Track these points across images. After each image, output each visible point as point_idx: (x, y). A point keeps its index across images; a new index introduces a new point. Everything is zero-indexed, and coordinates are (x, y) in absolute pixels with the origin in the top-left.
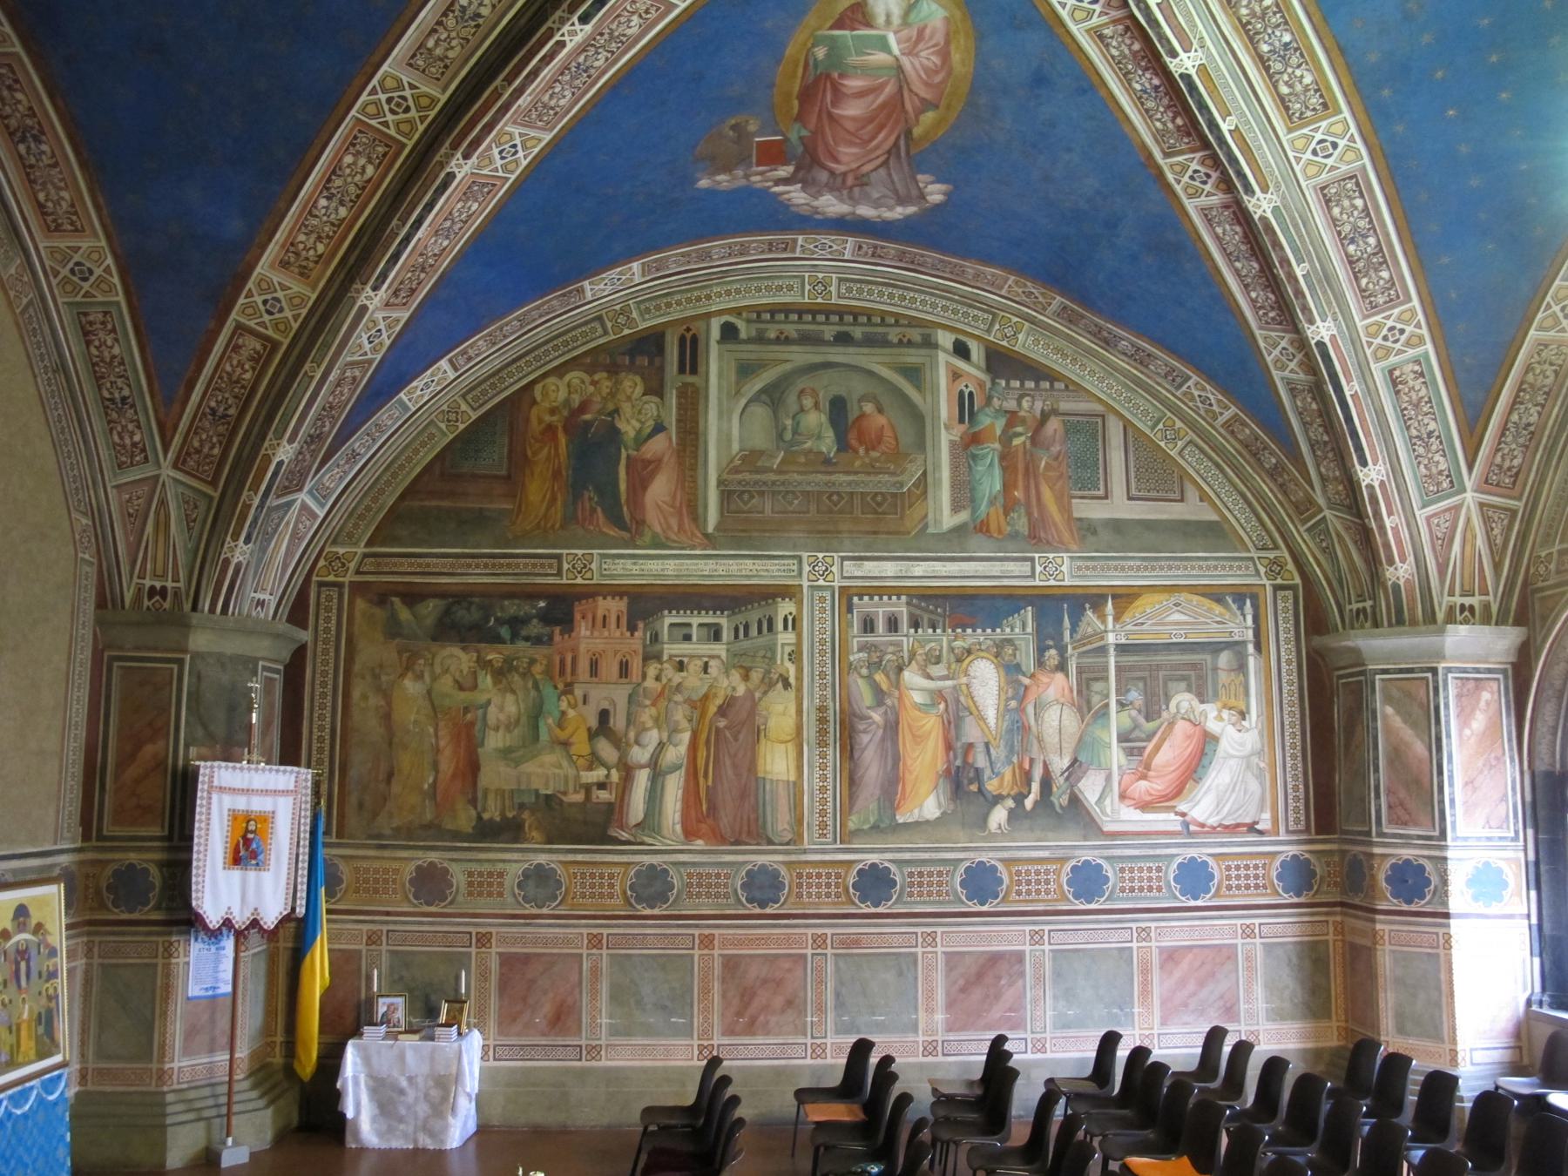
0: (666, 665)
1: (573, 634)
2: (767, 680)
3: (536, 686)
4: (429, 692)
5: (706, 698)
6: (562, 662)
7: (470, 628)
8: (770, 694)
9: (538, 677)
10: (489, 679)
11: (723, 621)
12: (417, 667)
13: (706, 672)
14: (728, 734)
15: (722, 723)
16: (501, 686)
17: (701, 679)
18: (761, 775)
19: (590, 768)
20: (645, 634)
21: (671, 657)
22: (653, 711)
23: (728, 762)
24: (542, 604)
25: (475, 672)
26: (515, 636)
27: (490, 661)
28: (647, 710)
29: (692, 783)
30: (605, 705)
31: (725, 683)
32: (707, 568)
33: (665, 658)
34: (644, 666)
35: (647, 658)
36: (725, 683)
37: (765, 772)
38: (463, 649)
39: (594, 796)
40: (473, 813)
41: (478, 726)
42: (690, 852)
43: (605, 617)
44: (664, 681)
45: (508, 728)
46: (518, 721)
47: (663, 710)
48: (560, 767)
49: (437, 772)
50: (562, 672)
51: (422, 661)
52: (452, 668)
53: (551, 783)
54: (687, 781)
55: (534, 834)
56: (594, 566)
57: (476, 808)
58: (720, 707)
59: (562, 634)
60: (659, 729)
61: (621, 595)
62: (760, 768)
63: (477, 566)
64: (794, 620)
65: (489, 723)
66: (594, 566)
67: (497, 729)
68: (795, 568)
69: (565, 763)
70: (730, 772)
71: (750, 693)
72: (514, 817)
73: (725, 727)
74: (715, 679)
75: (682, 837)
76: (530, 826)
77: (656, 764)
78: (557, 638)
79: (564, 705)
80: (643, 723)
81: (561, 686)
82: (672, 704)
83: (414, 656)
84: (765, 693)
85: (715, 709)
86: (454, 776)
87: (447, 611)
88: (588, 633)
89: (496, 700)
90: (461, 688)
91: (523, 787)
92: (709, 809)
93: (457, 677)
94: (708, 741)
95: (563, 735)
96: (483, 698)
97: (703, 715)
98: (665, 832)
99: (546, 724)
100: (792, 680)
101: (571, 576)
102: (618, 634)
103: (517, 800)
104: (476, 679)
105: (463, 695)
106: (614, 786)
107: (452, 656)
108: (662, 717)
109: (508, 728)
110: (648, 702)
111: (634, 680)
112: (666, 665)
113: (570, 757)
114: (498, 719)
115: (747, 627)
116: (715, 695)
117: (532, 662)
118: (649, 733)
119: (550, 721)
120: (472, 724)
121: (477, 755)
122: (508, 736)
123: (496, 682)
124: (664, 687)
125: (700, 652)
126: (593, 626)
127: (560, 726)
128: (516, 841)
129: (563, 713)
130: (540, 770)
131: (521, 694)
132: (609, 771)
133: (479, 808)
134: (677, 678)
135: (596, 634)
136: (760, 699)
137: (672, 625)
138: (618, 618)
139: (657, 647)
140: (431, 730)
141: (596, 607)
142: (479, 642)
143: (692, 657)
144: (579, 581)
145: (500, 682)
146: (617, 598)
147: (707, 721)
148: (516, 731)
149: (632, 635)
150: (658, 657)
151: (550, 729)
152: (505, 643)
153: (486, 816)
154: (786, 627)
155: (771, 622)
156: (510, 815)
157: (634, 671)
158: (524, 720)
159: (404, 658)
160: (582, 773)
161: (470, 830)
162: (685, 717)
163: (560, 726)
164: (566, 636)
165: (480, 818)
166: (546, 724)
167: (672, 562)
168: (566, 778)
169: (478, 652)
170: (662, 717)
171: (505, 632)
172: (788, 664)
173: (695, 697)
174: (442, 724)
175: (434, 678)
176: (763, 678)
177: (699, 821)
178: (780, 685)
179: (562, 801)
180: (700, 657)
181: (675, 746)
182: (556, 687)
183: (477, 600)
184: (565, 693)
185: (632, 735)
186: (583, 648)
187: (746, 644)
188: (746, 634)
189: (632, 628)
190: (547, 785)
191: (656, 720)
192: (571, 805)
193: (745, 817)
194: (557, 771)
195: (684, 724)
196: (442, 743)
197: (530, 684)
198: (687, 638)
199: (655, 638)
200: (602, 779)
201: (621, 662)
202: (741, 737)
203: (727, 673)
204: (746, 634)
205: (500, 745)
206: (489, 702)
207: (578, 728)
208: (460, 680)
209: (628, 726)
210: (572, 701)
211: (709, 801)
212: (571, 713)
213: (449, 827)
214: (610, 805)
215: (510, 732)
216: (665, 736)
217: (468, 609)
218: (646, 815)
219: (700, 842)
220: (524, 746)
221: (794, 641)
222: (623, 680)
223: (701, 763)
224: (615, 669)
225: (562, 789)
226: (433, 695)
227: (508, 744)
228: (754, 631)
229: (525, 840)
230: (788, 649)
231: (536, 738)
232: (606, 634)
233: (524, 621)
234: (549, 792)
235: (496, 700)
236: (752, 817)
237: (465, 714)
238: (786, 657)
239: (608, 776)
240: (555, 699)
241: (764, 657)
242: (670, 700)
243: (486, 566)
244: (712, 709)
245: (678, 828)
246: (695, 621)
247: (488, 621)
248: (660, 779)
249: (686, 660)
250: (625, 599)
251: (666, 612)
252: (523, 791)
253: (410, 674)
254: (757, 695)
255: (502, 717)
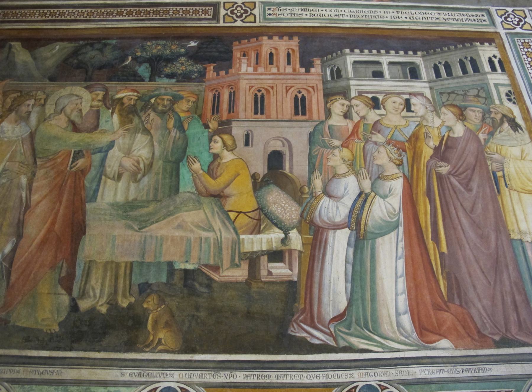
0: (354, 102)
1: (232, 71)
2: (488, 121)
3: (180, 126)
4: (32, 136)
5: (415, 138)
6: (217, 100)
7: (100, 68)
8: (497, 135)
9: (182, 115)
10: (116, 118)
11: (418, 60)
12: (24, 109)
13: (409, 110)
14: (453, 180)
15: (445, 169)
16: (128, 126)
17: (404, 117)
18: (515, 236)
19: (257, 230)
20: (324, 70)
21: (360, 94)
22: (346, 153)
23: (465, 221)
24: (193, 44)
25: (98, 112)
26: (155, 74)
27: (121, 99)
28: (336, 151)
29: (417, 250)
30: (277, 146)
31: (437, 122)
32: (389, 15)
33: (353, 94)
34: (326, 103)
35: (328, 95)
36: (437, 122)
37: (520, 232)
38: (87, 88)
39: (264, 272)
40: (65, 299)
41: (92, 173)
42: (432, 361)
43: (271, 55)
44: (356, 119)
45: (135, 177)
46: (151, 165)
47: (359, 153)
48: (210, 229)
49: (19, 236)
50: (216, 108)
51: (32, 102)
52: (68, 110)
53: (195, 253)
54: (409, 245)
55: (161, 335)
56: (256, 12)
57: (69, 290)
58: (437, 149)
59: (217, 70)
60: (357, 175)
61: (291, 36)
62: (512, 226)
63: (120, 14)
64: (500, 62)
65: (108, 170)
66: (256, 12)
67: (119, 176)
68: (485, 18)
69: (217, 224)
70: (471, 233)
71: (472, 134)
72: (130, 306)
73: (449, 173)
74: (423, 117)
75: (415, 335)
76: (156, 322)
77: (358, 223)
78: (211, 73)
79: (217, 146)
80: (333, 167)
81: (213, 125)
82: (370, 146)
83: (24, 95)
84: (491, 134)
85: (431, 152)
86: (44, 242)
87: (76, 53)
88: (251, 70)
89: (121, 141)
90: (76, 128)
91: (148, 259)
92: (449, 288)
93: (73, 117)
94: (429, 193)
95: (213, 185)
96: (104, 140)
97: (416, 157)
98: (386, 328)
99: (191, 170)
100: (519, 120)
101: (228, 19)
102: (289, 69)
103: (137, 280)
104: (98, 119)
105: (76, 137)
106: (296, 255)
107: (71, 95)
108: (360, 161)
109: (135, 177)
110: (336, 143)
111: (315, 117)
112: (354, 102)
113: (226, 213)
114: (121, 165)
115: (447, 67)
116: (427, 136)
117: (176, 99)
118: (343, 181)
119: (196, 166)
120: (83, 172)
121: (84, 213)
122: (133, 186)
123: (122, 124)
124: (356, 126)
125: (399, 89)
126: (257, 62)
127: (211, 172)
128: (130, 346)
129: (216, 156)
130: (178, 233)
131: (157, 135)
132: (286, 232)
133: (75, 294)
134: (373, 116)
135: (261, 70)
136: (487, 141)
137: (355, 62)
138: (289, 55)
139: (342, 83)
140: (24, 180)
141: (261, 46)
142: (110, 79)
143: (388, 94)
144: (239, 23)
145: (131, 122)
146: (286, 38)
147: (423, 167)
148: (146, 180)
149: (308, 71)
150: (345, 93)
151: (195, 175)
152: (143, 80)
153: (84, 305)
154: (493, 68)
155: (473, 62)
156: (124, 303)
157: (314, 107)
158: (159, 165)
159: (9, 101)
160: (242, 237)
161: (56, 328)
162: (391, 160)
163: (211, 172)
164: (222, 73)
165: (74, 307)
166: (191, 170)
167: (347, 10)
168: (219, 245)
169: (106, 90)
170: (360, 161)
171: (143, 70)
172: (510, 105)
173: (401, 138)
174: (40, 173)
175: (43, 119)
176: (483, 119)
177: (438, 308)
178: (506, 125)
179: (210, 279)
180: (398, 94)
181: (384, 197)
182: (207, 126)
183: (114, 42)
184: (218, 132)
185: (318, 183)
186: (243, 84)
187: (451, 83)
188: (449, 73)
189: (307, 65)
190: (187, 256)
191: (352, 165)
192: (227, 285)
193: (509, 300)
194: (204, 234)
195: (392, 169)
196: (35, 198)
197: (171, 123)
198: (378, 75)
199: (338, 74)
200: (276, 245)
201: (296, 98)
202: (474, 185)
203: (437, 112)
204: (449, 73)
205: (120, 198)
206: (111, 145)
207: (238, 175)
208: (77, 120)
209: (311, 171)
210: (229, 142)
211: (448, 277)
212: (228, 157)
213: (23, 323)
214: (292, 285)
215: (137, 181)
216: (367, 185)
217: (101, 51)
218: (350, 303)
219: (444, 343)
220: (156, 200)
221: (507, 82)
222: (300, 117)
223: (425, 220)
224: (288, 105)
225: (212, 262)
226: (37, 140)
227: (131, 198)
228: (457, 71)
229: (148, 346)
230: (503, 90)
231: (175, 189)
232: (274, 70)
233: (170, 60)
234: (190, 267)
235: (121, 141)
236: (518, 298)
237: (75, 159)
238: (504, 98)
239: (284, 241)
240: (205, 140)
241: (478, 96)
242: (367, 141)
243: (129, 13)
244: (427, 152)
245: (406, 320)
246: (385, 60)
247: (123, 59)
248: (368, 245)
249: (381, 97)
250: (296, 39)
251: (347, 51)
252: (149, 264)
253: (13, 115)
254: (482, 136)
255: (128, 163)
